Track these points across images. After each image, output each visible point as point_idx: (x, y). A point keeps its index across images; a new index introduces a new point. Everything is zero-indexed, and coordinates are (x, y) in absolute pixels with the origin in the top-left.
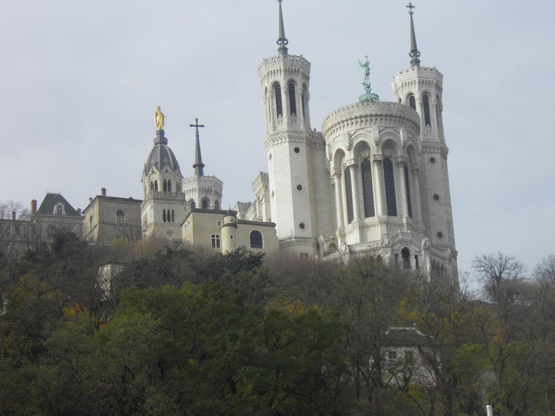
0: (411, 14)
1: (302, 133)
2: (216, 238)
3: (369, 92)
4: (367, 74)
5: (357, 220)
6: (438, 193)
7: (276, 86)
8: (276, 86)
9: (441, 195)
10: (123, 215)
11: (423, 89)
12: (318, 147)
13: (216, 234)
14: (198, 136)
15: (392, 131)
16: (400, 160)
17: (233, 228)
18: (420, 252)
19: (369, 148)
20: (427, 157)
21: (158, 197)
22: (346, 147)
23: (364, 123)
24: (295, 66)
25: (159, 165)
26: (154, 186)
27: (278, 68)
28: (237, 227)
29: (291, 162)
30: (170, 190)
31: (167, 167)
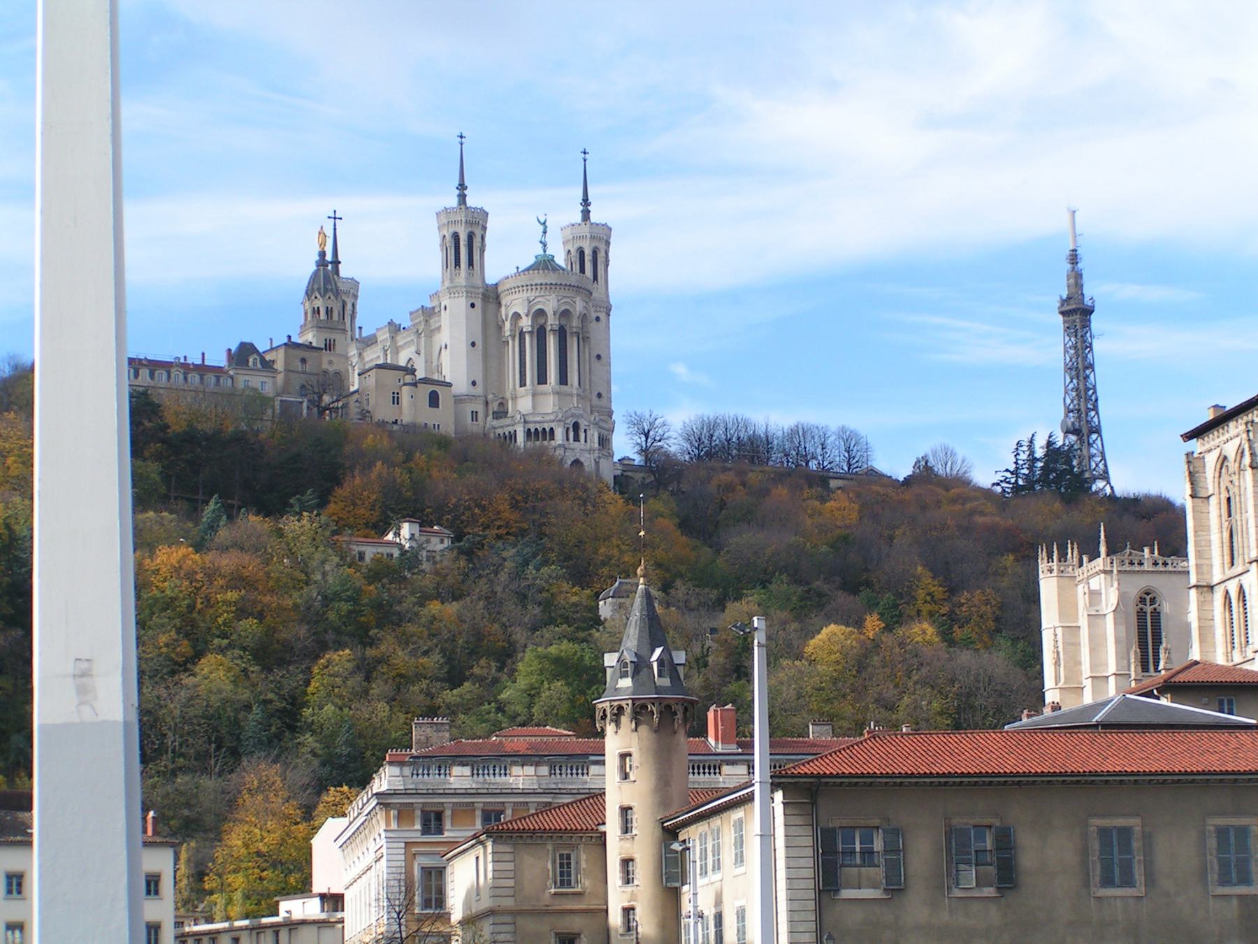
0: (585, 160)
1: (478, 288)
2: (396, 395)
3: (545, 251)
4: (545, 232)
6: (600, 353)
7: (456, 237)
8: (456, 237)
9: (602, 356)
11: (594, 245)
12: (491, 300)
13: (396, 391)
14: (335, 229)
15: (568, 300)
16: (575, 330)
17: (413, 388)
19: (546, 315)
20: (594, 315)
21: (321, 325)
23: (543, 291)
28: (417, 387)
29: (467, 318)
30: (331, 318)
31: (330, 294)
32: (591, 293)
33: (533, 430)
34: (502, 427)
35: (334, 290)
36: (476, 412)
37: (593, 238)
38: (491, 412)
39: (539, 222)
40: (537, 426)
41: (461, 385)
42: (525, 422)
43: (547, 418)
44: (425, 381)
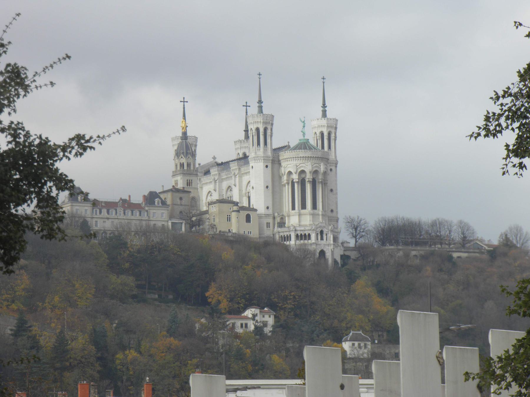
0: (324, 83)
1: (270, 157)
4: (304, 127)
5: (298, 211)
10: (182, 200)
11: (329, 130)
12: (276, 162)
14: (184, 108)
17: (238, 213)
18: (328, 232)
21: (185, 173)
22: (294, 172)
24: (268, 120)
25: (185, 154)
26: (182, 165)
27: (260, 121)
28: (239, 212)
32: (328, 159)
33: (299, 235)
34: (283, 232)
35: (191, 153)
36: (269, 223)
37: (328, 127)
38: (276, 223)
39: (301, 121)
40: (302, 232)
41: (261, 209)
42: (296, 230)
43: (307, 228)
44: (243, 208)
